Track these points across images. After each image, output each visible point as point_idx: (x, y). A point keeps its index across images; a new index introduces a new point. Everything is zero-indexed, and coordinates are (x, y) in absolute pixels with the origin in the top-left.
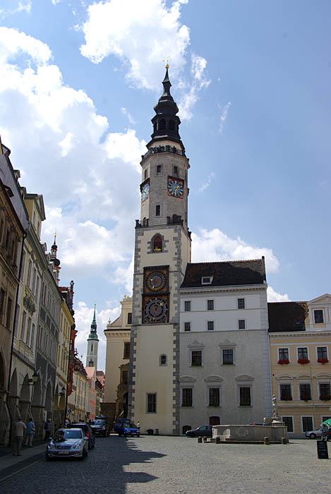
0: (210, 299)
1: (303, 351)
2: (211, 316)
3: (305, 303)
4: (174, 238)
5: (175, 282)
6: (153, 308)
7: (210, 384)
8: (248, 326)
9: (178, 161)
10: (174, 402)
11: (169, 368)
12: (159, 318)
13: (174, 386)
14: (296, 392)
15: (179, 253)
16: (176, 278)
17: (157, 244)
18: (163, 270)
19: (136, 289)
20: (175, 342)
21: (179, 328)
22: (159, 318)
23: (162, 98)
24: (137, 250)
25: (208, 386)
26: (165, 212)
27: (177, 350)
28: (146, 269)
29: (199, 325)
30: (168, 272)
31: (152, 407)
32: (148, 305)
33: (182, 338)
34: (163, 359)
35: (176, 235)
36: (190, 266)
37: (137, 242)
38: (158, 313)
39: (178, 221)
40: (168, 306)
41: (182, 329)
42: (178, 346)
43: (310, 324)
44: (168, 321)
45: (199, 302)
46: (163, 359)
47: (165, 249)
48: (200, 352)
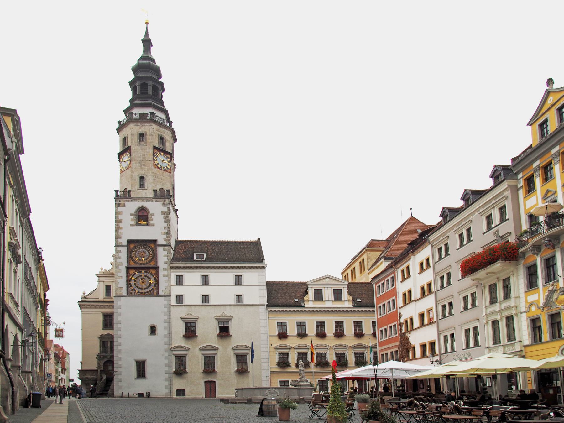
1: (301, 325)
2: (205, 290)
4: (163, 213)
5: (165, 256)
8: (246, 301)
12: (147, 290)
17: (142, 217)
21: (169, 300)
22: (147, 290)
23: (142, 58)
28: (129, 242)
34: (153, 330)
35: (165, 209)
40: (157, 280)
41: (173, 301)
45: (192, 277)
46: (153, 330)
47: (152, 222)
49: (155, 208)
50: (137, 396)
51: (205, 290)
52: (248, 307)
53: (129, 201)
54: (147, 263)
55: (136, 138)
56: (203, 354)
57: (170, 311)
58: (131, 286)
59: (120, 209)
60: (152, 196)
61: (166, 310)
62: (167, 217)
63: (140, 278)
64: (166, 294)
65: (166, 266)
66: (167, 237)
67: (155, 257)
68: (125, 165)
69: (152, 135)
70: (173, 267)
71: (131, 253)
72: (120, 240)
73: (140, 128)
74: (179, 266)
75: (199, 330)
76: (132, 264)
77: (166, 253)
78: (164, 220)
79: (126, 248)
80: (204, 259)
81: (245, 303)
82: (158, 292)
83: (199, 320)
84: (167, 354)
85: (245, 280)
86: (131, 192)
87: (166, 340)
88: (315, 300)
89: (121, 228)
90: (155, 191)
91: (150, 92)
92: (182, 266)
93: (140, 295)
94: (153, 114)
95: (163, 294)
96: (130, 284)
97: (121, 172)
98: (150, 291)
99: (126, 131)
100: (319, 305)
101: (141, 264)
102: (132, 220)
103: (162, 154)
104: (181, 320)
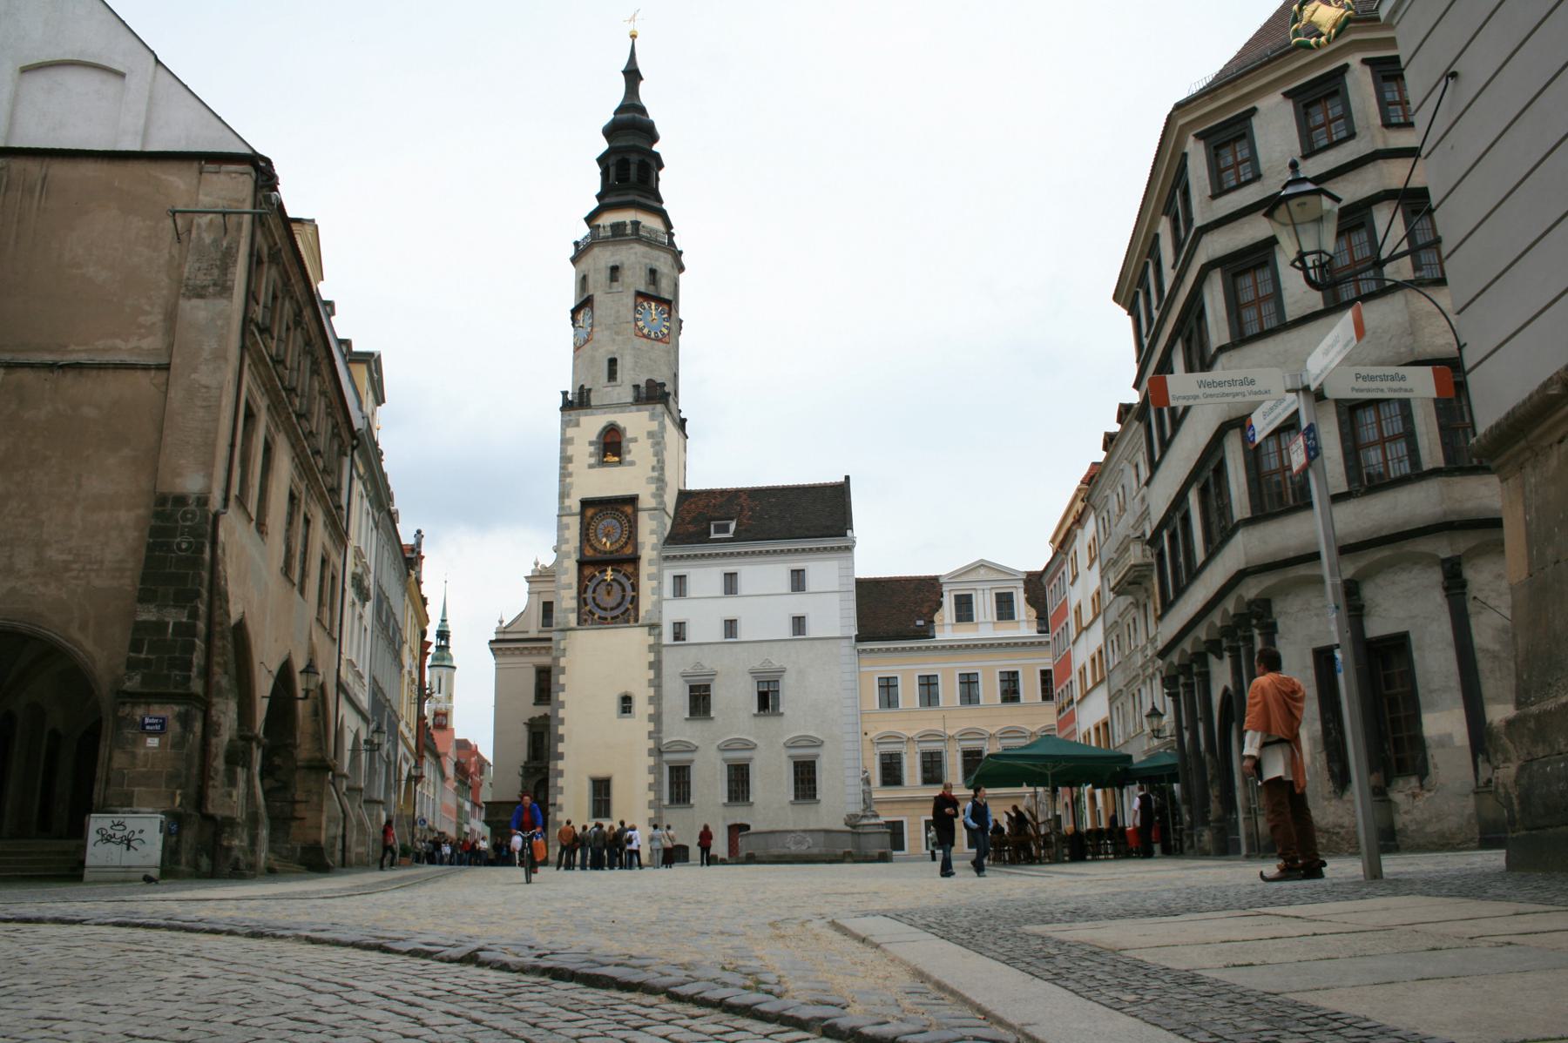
2: (730, 607)
3: (936, 579)
4: (651, 435)
6: (602, 589)
7: (729, 755)
8: (813, 630)
9: (663, 262)
10: (651, 796)
11: (639, 723)
12: (615, 613)
13: (651, 761)
15: (660, 467)
16: (653, 524)
17: (611, 445)
19: (564, 548)
20: (651, 665)
21: (660, 634)
22: (615, 613)
23: (620, 110)
24: (566, 460)
25: (725, 760)
26: (629, 375)
27: (657, 683)
28: (586, 504)
30: (636, 510)
32: (591, 586)
33: (668, 657)
34: (626, 703)
35: (654, 426)
36: (685, 496)
37: (565, 442)
38: (611, 601)
39: (657, 394)
40: (635, 587)
41: (667, 637)
42: (658, 675)
43: (947, 629)
44: (636, 620)
45: (705, 577)
46: (626, 703)
47: (628, 458)
48: (707, 688)
51: (730, 607)
55: (605, 275)
56: (725, 760)
59: (570, 432)
60: (630, 400)
62: (658, 444)
63: (603, 586)
68: (583, 333)
72: (567, 502)
75: (718, 697)
76: (589, 553)
79: (578, 519)
85: (811, 582)
89: (570, 475)
90: (636, 387)
94: (636, 224)
97: (577, 348)
99: (587, 262)
102: (591, 455)
104: (681, 681)
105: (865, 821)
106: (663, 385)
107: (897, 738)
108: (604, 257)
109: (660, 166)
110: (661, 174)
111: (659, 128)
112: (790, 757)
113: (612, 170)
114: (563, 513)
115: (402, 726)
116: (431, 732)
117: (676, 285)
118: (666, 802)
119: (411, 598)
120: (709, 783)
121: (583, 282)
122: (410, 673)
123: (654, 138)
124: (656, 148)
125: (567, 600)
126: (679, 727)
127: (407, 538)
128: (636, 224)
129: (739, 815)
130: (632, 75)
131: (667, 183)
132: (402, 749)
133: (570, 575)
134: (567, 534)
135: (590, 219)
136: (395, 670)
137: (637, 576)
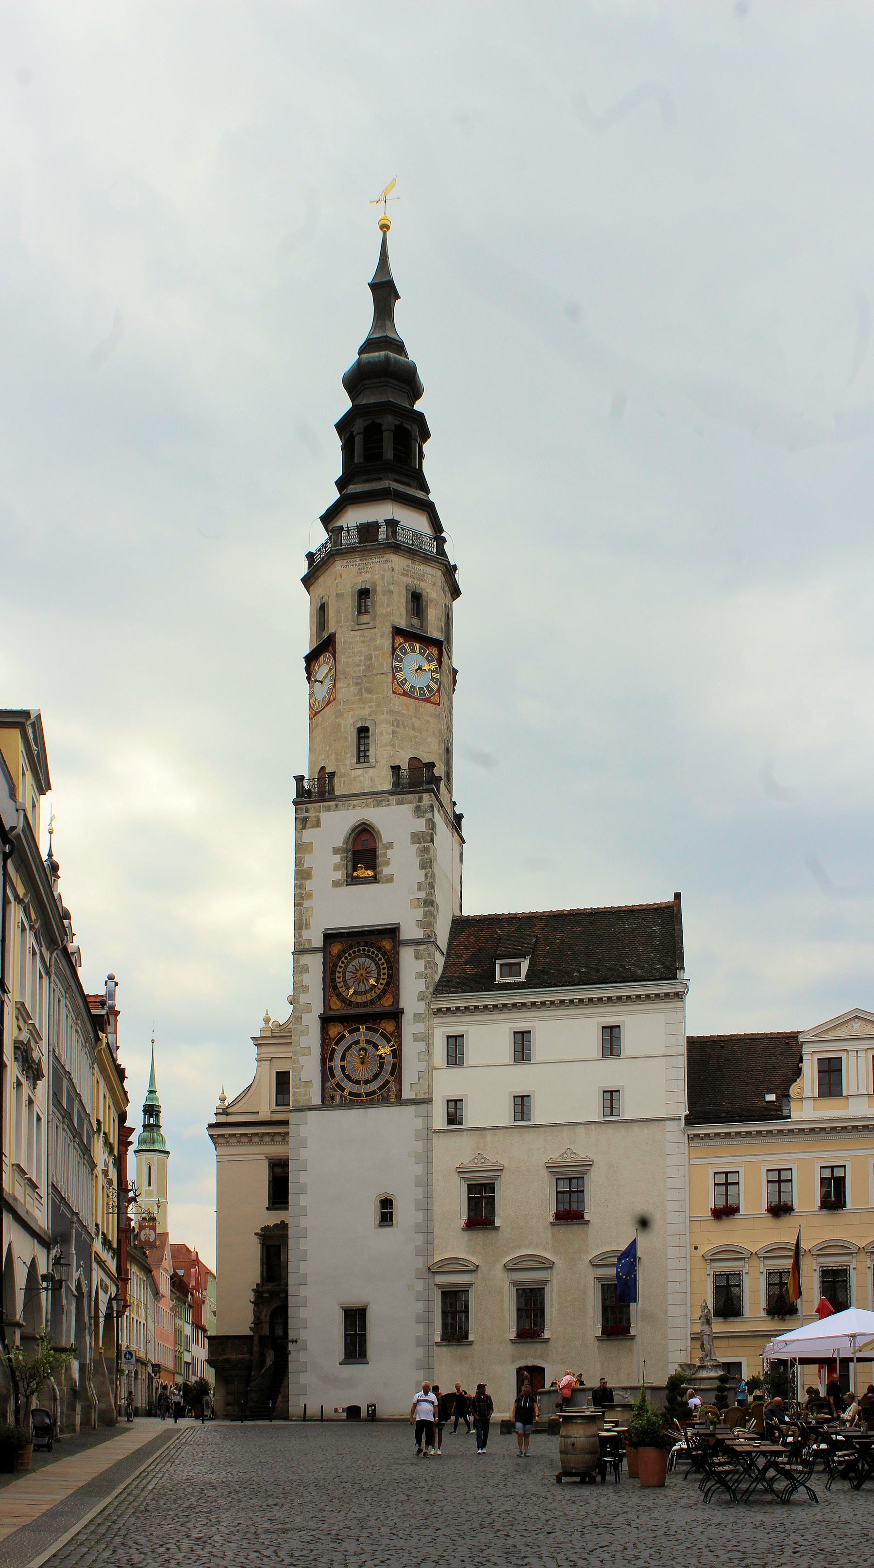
0: (522, 1026)
1: (780, 1179)
2: (522, 1079)
4: (416, 838)
5: (419, 975)
8: (629, 1110)
14: (754, 1295)
17: (363, 854)
18: (381, 942)
21: (429, 1116)
23: (369, 346)
24: (302, 874)
28: (330, 937)
29: (488, 1108)
31: (355, 1347)
34: (386, 1211)
35: (420, 825)
36: (462, 926)
37: (301, 848)
38: (364, 1073)
39: (422, 780)
40: (397, 1053)
43: (806, 1106)
45: (488, 1038)
46: (386, 1211)
47: (386, 871)
48: (491, 1187)
49: (395, 822)
50: (344, 1415)
51: (522, 1079)
52: (636, 1128)
53: (328, 809)
54: (372, 1002)
55: (349, 604)
56: (513, 1283)
57: (428, 1150)
58: (333, 1076)
59: (309, 835)
60: (387, 786)
61: (419, 1146)
62: (426, 850)
63: (354, 1050)
64: (422, 1096)
65: (421, 1007)
66: (425, 915)
67: (392, 982)
68: (322, 691)
69: (391, 592)
70: (439, 1010)
71: (333, 972)
72: (306, 934)
73: (360, 572)
74: (453, 1005)
77: (420, 965)
78: (417, 860)
79: (319, 958)
80: (522, 978)
81: (627, 1115)
82: (400, 1090)
83: (505, 1176)
84: (420, 1285)
85: (629, 1042)
86: (336, 780)
87: (419, 1240)
88: (822, 1095)
90: (396, 769)
91: (389, 454)
92: (462, 1004)
93: (355, 1101)
95: (412, 1096)
96: (331, 1068)
97: (314, 714)
98: (381, 1088)
100: (830, 1111)
101: (358, 1005)
102: (336, 868)
103: (417, 646)
104: (456, 1178)
105: (704, 1374)
106: (431, 765)
107: (738, 1254)
108: (346, 575)
109: (425, 435)
110: (426, 447)
111: (424, 376)
112: (598, 1279)
113: (358, 440)
114: (300, 951)
115: (97, 1245)
116: (136, 1247)
117: (448, 618)
118: (438, 1339)
119: (103, 1070)
120: (493, 1313)
121: (321, 612)
122: (105, 1173)
123: (416, 392)
124: (418, 406)
125: (308, 1072)
126: (454, 1242)
127: (92, 983)
128: (392, 524)
129: (531, 1356)
130: (384, 292)
131: (436, 462)
132: (97, 1275)
133: (311, 1038)
134: (307, 979)
135: (329, 518)
136: (84, 1170)
137: (399, 1036)
